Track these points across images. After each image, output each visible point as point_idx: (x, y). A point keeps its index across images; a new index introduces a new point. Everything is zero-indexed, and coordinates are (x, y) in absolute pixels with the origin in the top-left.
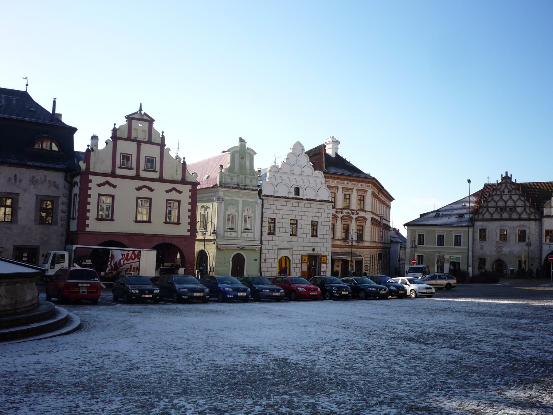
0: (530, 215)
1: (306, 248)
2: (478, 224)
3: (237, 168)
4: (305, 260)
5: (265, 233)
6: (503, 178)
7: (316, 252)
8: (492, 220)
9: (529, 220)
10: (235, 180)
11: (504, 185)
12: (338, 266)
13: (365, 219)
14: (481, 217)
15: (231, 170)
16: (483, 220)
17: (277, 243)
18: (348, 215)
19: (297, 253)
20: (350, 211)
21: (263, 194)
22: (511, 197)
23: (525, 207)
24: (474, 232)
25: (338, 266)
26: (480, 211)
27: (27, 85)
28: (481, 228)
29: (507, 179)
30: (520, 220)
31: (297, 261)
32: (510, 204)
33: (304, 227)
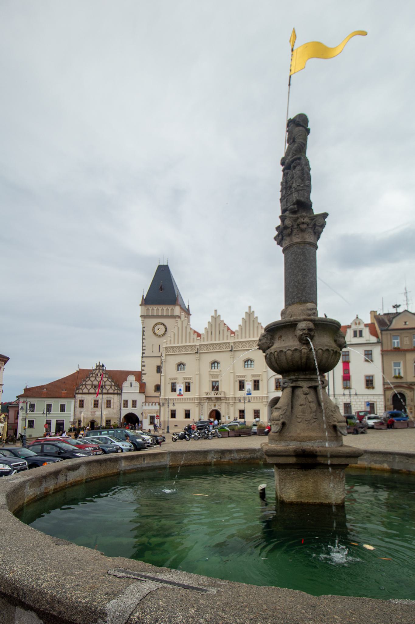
0: (114, 391)
2: (79, 397)
8: (89, 393)
9: (114, 394)
11: (97, 371)
14: (81, 391)
16: (82, 394)
23: (111, 385)
24: (75, 402)
26: (81, 387)
28: (80, 399)
29: (100, 367)
30: (108, 393)
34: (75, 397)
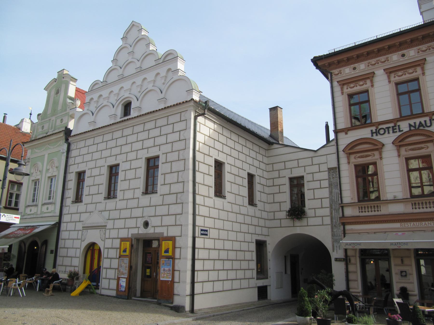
1: (131, 223)
4: (125, 251)
5: (68, 201)
7: (150, 230)
12: (404, 274)
17: (84, 217)
18: (415, 131)
19: (114, 233)
20: (422, 120)
21: (72, 134)
25: (404, 274)
27: (31, 114)
31: (113, 253)
33: (130, 174)
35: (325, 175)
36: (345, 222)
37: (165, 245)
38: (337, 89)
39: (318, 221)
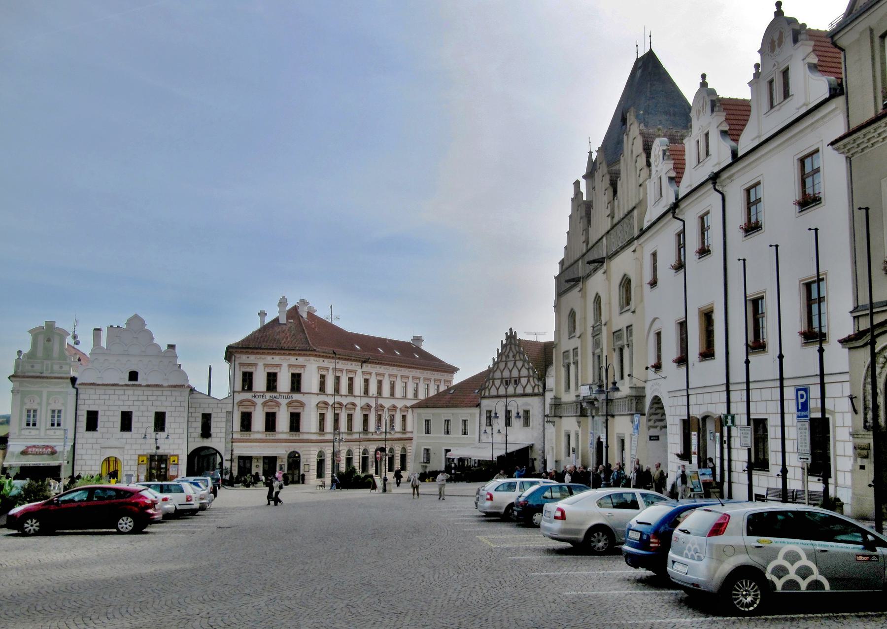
2: (486, 404)
3: (40, 353)
6: (508, 338)
7: (161, 452)
8: (498, 396)
10: (38, 367)
11: (508, 347)
12: (257, 466)
13: (302, 405)
15: (32, 355)
17: (99, 441)
19: (132, 452)
20: (276, 395)
21: (78, 382)
22: (515, 363)
23: (529, 377)
25: (257, 466)
30: (525, 395)
32: (515, 373)
34: (478, 405)
35: (224, 415)
36: (233, 441)
37: (172, 459)
38: (237, 366)
39: (218, 440)
